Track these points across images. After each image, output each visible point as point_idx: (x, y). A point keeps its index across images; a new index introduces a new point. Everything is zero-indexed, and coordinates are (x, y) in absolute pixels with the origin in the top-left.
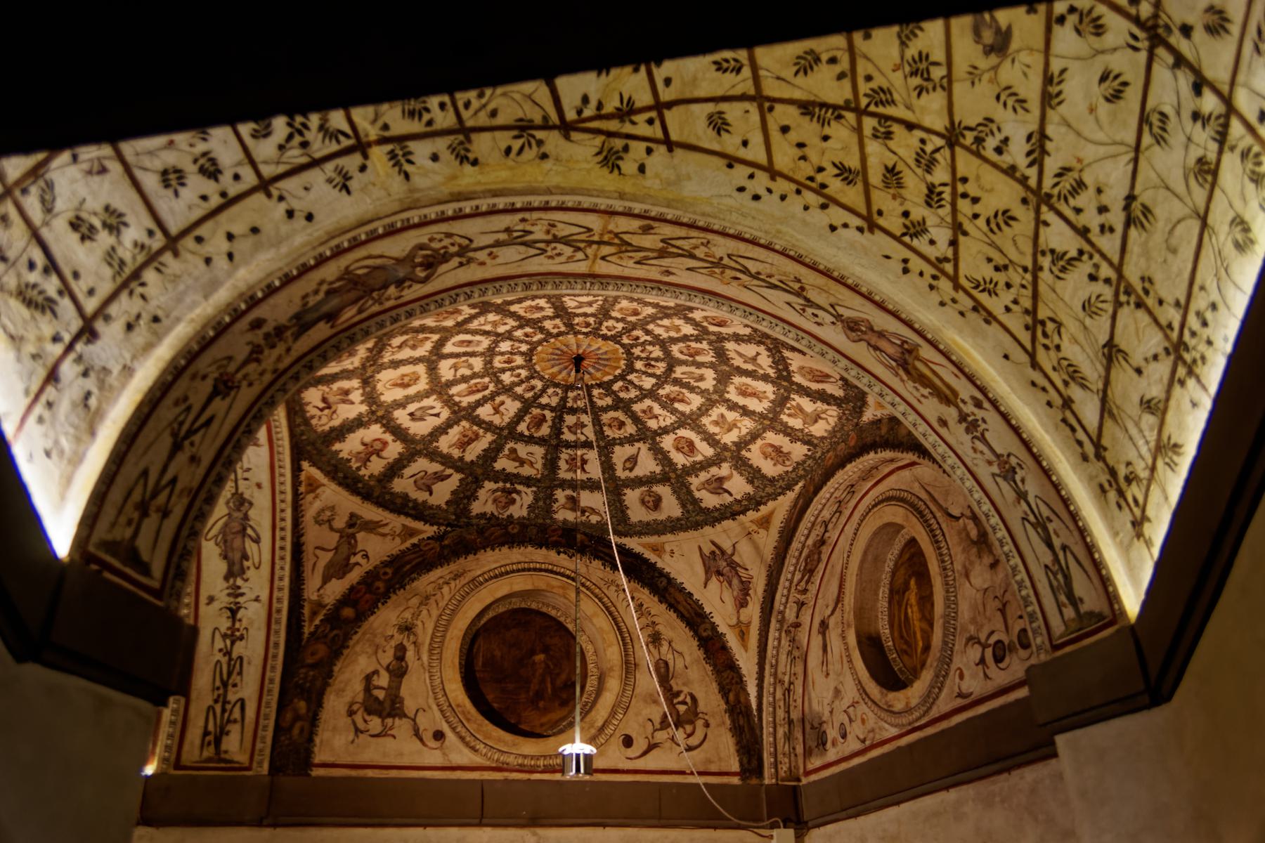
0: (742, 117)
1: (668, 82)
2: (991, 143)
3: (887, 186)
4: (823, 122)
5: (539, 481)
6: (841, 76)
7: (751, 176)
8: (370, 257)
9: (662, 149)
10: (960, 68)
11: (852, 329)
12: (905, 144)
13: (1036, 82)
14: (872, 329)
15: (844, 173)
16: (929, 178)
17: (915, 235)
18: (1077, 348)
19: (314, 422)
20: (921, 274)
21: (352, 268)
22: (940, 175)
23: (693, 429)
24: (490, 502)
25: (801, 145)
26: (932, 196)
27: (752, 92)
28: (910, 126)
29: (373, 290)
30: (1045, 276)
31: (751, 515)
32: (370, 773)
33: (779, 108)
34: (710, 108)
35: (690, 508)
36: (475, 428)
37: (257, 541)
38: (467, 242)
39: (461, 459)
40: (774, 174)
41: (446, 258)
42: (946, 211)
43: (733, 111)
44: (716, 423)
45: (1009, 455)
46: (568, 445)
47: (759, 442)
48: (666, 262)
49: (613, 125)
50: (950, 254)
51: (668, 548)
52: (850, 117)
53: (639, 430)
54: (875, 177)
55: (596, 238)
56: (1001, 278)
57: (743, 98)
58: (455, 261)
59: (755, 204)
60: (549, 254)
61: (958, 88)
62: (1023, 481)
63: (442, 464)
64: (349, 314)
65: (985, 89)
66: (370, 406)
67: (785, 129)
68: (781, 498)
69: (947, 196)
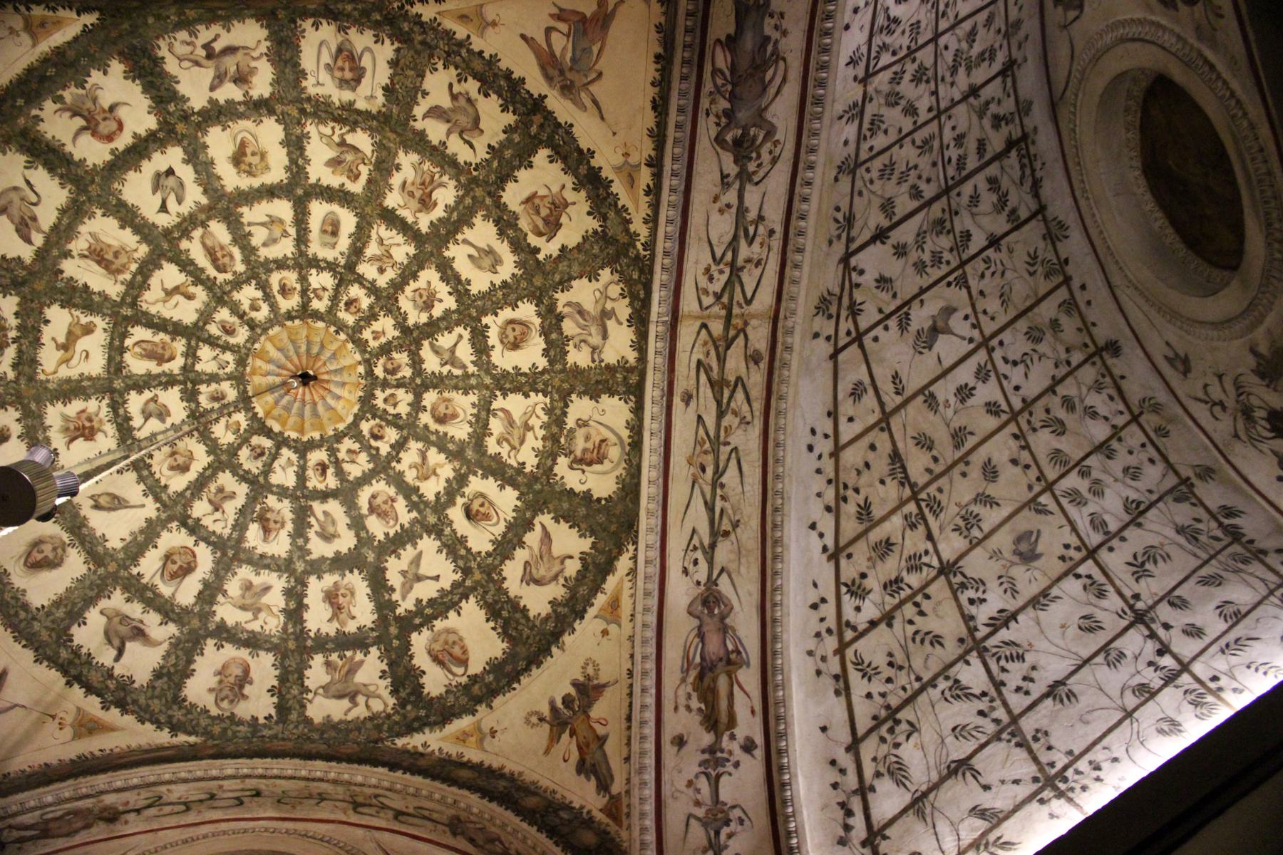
0: (867, 411)
1: (876, 339)
2: (971, 593)
3: (875, 547)
4: (892, 474)
5: (31, 379)
6: (929, 471)
7: (826, 436)
8: (784, 80)
9: (831, 350)
10: (993, 543)
11: (705, 603)
12: (915, 542)
13: (1035, 589)
14: (723, 618)
15: (865, 511)
16: (904, 574)
17: (853, 594)
18: (920, 754)
19: (183, 35)
20: (822, 620)
21: (781, 63)
22: (914, 580)
23: (217, 562)
25: (867, 465)
26: (893, 585)
27: (888, 410)
28: (930, 537)
29: (734, 85)
30: (934, 693)
31: (93, 705)
32: (1244, 10)
33: (885, 435)
34: (867, 380)
35: (60, 613)
36: (134, 267)
38: (756, 179)
39: (67, 254)
40: (835, 454)
41: (740, 159)
42: (890, 602)
43: (869, 400)
44: (248, 586)
45: (734, 807)
46: (117, 406)
47: (244, 653)
48: (706, 392)
49: (845, 301)
50: (861, 628)
52: (907, 492)
53: (181, 495)
54: (876, 535)
55: (736, 310)
56: (889, 672)
57: (882, 404)
58: (731, 169)
59: (804, 448)
60: (713, 267)
61: (978, 551)
62: (730, 836)
63: (55, 228)
64: (722, 60)
65: (996, 567)
66: (199, 113)
67: (873, 447)
69: (903, 594)
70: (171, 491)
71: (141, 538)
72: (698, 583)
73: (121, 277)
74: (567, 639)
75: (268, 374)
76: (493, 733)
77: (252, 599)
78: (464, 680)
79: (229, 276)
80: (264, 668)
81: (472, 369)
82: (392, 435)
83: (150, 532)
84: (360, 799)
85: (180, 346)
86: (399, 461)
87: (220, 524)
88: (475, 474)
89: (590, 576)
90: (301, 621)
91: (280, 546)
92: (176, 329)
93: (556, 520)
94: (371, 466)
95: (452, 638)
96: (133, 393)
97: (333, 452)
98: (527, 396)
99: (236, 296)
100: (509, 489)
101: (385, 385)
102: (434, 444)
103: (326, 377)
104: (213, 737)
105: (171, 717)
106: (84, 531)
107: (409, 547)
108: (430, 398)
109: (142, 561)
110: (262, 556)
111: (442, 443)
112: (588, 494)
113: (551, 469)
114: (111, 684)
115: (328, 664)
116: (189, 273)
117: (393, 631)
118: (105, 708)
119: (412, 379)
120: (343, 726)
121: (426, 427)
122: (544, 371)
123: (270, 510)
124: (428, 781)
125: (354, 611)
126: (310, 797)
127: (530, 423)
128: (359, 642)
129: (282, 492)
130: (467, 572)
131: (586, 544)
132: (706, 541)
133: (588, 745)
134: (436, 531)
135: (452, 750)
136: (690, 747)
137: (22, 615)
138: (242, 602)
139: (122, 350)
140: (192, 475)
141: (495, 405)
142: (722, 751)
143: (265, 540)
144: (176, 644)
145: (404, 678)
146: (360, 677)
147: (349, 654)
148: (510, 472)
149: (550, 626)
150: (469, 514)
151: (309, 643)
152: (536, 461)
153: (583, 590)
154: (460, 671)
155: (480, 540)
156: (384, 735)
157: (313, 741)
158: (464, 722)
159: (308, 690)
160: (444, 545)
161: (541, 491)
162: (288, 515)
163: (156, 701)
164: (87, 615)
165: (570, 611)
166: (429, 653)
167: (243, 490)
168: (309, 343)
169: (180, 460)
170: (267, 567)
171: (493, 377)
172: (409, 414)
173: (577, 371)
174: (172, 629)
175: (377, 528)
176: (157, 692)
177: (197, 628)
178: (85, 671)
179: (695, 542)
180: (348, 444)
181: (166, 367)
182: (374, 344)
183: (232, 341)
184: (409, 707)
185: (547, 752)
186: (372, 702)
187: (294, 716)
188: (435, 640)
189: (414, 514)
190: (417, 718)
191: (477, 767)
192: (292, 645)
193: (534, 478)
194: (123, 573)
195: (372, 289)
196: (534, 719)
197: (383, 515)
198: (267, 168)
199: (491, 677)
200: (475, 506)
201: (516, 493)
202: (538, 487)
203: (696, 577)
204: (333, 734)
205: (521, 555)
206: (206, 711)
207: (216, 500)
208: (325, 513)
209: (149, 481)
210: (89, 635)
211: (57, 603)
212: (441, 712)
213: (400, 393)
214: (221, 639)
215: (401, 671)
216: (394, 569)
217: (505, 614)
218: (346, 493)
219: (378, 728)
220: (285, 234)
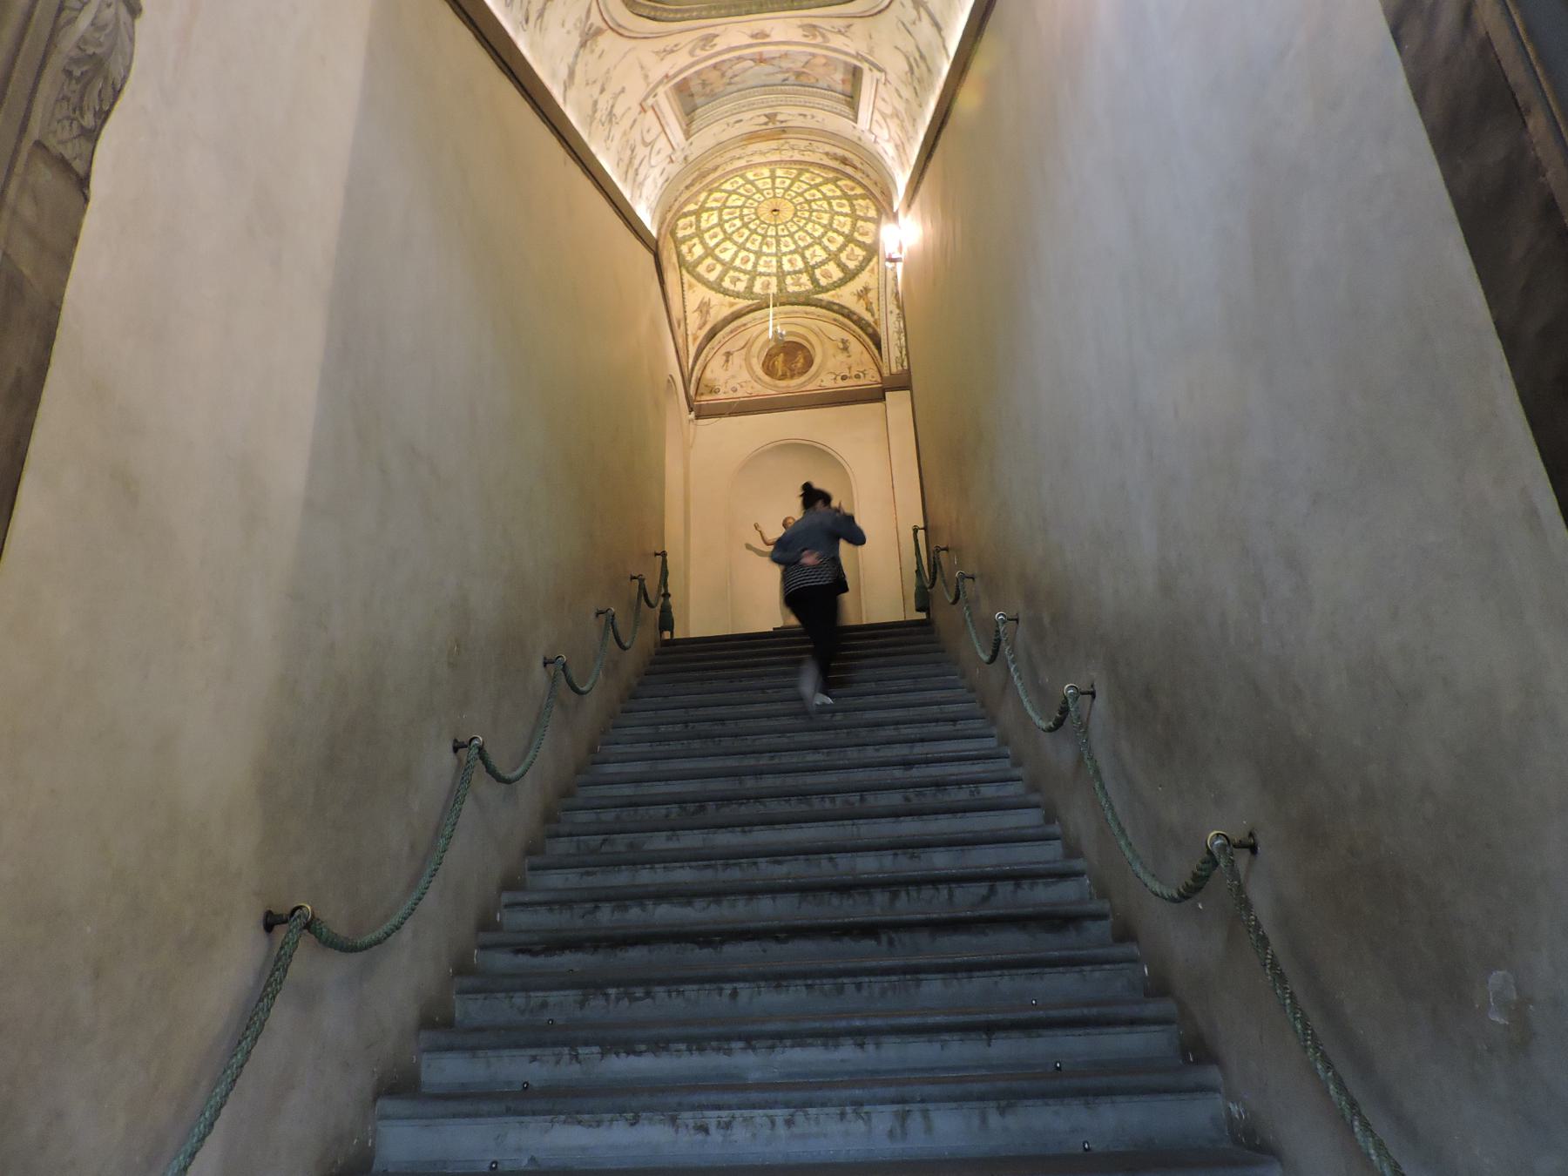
77: (767, 264)
80: (774, 281)
83: (736, 254)
87: (755, 247)
91: (773, 249)
117: (810, 269)
128: (800, 272)
134: (820, 244)
145: (814, 281)
155: (833, 247)
165: (860, 269)
175: (802, 244)
177: (753, 275)
210: (727, 283)
212: (826, 290)
216: (808, 253)
218: (791, 235)
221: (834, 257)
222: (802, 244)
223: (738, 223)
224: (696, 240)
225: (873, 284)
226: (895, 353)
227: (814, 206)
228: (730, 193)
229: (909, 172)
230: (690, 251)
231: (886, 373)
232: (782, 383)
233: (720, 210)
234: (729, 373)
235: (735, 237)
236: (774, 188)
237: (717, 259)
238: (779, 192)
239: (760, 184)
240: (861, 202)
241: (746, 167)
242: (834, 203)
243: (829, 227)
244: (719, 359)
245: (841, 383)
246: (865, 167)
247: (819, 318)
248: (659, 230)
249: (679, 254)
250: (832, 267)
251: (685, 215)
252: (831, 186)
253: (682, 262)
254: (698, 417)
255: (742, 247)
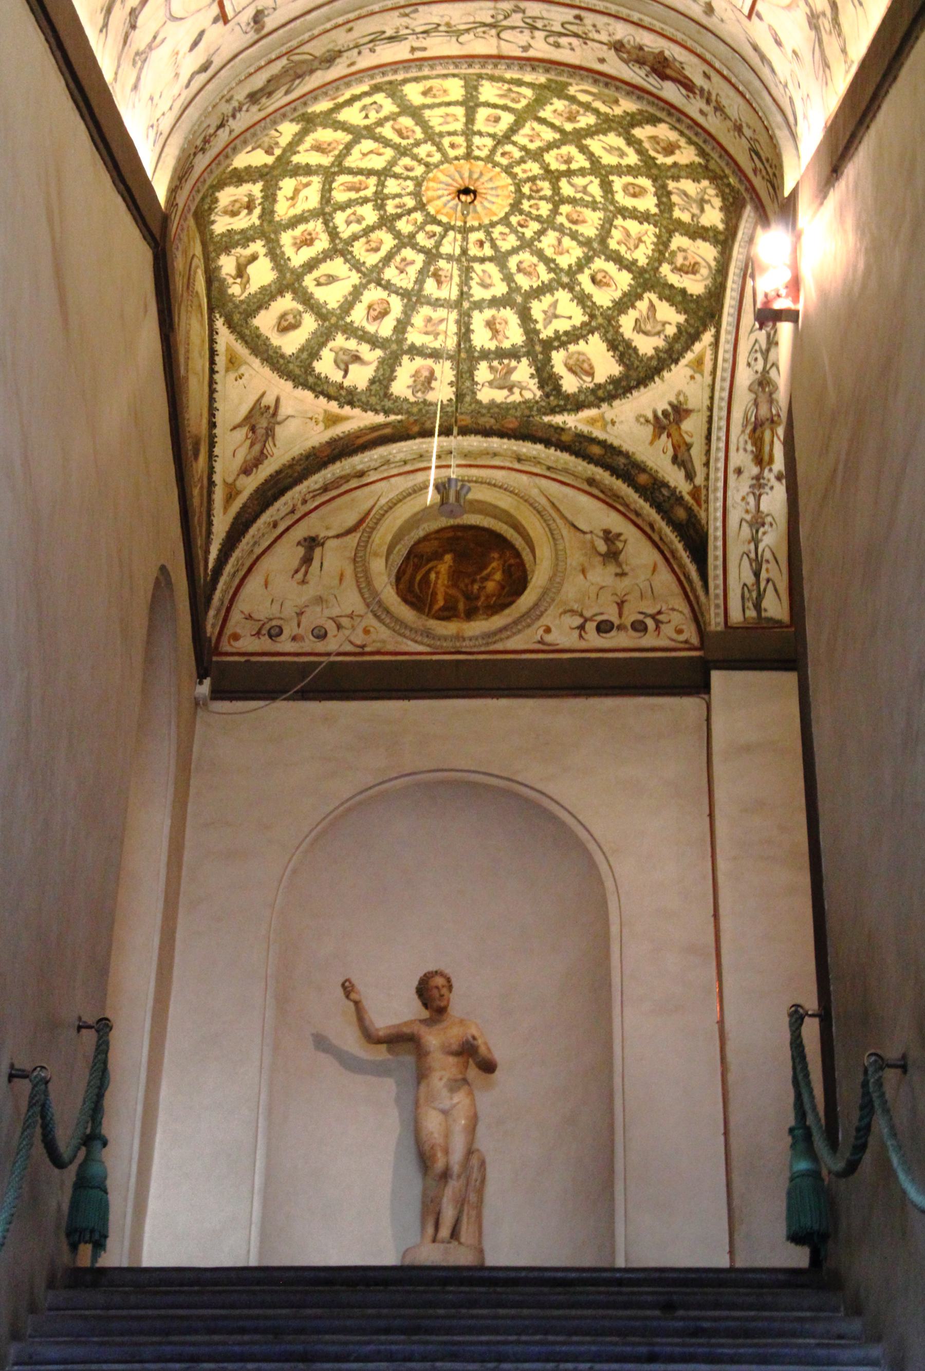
5: (271, 222)
14: (771, 394)
23: (405, 306)
24: (233, 198)
31: (333, 406)
35: (305, 355)
36: (341, 147)
37: (287, 93)
45: (768, 515)
47: (430, 362)
51: (243, 369)
53: (376, 265)
62: (764, 533)
68: (370, 414)
70: (368, 265)
71: (350, 298)
72: (757, 372)
73: (332, 154)
74: (665, 374)
75: (439, 189)
76: (613, 423)
78: (591, 386)
79: (411, 141)
80: (445, 372)
81: (599, 199)
82: (535, 226)
83: (356, 293)
84: (523, 457)
85: (373, 180)
86: (540, 241)
87: (406, 281)
88: (600, 257)
89: (683, 339)
90: (470, 341)
92: (370, 173)
93: (660, 299)
94: (518, 243)
95: (581, 358)
96: (339, 213)
97: (488, 233)
98: (641, 223)
99: (415, 150)
100: (625, 272)
101: (530, 198)
102: (567, 235)
103: (484, 191)
104: (413, 415)
105: (384, 406)
106: (312, 301)
107: (548, 295)
108: (565, 209)
109: (352, 312)
110: (437, 300)
111: (574, 236)
112: (683, 291)
113: (657, 269)
114: (343, 393)
115: (491, 368)
116: (382, 143)
118: (341, 407)
119: (552, 196)
120: (504, 406)
121: (562, 224)
122: (655, 215)
123: (441, 269)
124: (573, 458)
125: (507, 334)
126: (488, 454)
127: (644, 239)
128: (514, 354)
129: (450, 258)
130: (592, 316)
131: (681, 318)
132: (764, 347)
133: (679, 447)
135: (585, 429)
136: (745, 475)
137: (281, 361)
138: (425, 330)
139: (330, 190)
140: (382, 253)
141: (616, 222)
142: (764, 478)
143: (439, 288)
144: (382, 362)
145: (547, 379)
146: (515, 377)
147: (506, 361)
148: (626, 262)
149: (654, 363)
150: (594, 280)
151: (476, 354)
152: (647, 261)
153: (678, 346)
154: (589, 379)
156: (534, 413)
157: (483, 415)
158: (592, 412)
159: (477, 384)
160: (575, 297)
161: (650, 278)
162: (456, 273)
163: (373, 398)
164: (321, 353)
166: (566, 365)
167: (420, 259)
168: (471, 173)
169: (373, 245)
170: (442, 306)
171: (615, 207)
172: (548, 216)
173: (679, 222)
174: (379, 353)
175: (524, 283)
176: (373, 393)
177: (395, 351)
178: (325, 388)
179: (757, 347)
180: (500, 228)
181: (362, 194)
182: (522, 175)
183: (411, 174)
184: (552, 398)
185: (651, 443)
186: (524, 392)
187: (468, 399)
188: (570, 357)
189: (552, 275)
190: (558, 406)
191: (603, 444)
192: (463, 355)
193: (642, 271)
194: (341, 323)
195: (523, 148)
196: (642, 420)
197: (528, 274)
198: (448, 95)
199: (611, 387)
200: (599, 277)
201: (631, 276)
202: (647, 276)
203: (756, 368)
204: (497, 410)
205: (633, 314)
206: (406, 400)
207: (402, 266)
208: (484, 271)
209: (352, 262)
210: (325, 366)
211: (302, 350)
212: (576, 404)
213: (542, 204)
214: (412, 355)
215: (545, 375)
216: (537, 309)
217: (621, 348)
218: (500, 259)
219: (531, 409)
220: (457, 120)
221: (602, 322)
222: (524, 283)
223: (370, 215)
224: (258, 247)
225: (696, 397)
226: (740, 574)
227: (566, 189)
228: (358, 134)
229: (842, 80)
230: (241, 272)
231: (715, 622)
232: (449, 628)
233: (329, 175)
234: (311, 591)
235: (359, 249)
236: (469, 132)
237: (307, 300)
238: (482, 145)
239: (434, 118)
240: (688, 185)
241: (405, 64)
242: (618, 183)
243: (599, 246)
244: (287, 554)
245: (594, 639)
246: (717, 86)
247: (551, 473)
248: (173, 191)
249: (212, 276)
250: (595, 348)
251: (240, 177)
252: (614, 140)
253: (217, 299)
254: (218, 694)
255: (372, 276)
